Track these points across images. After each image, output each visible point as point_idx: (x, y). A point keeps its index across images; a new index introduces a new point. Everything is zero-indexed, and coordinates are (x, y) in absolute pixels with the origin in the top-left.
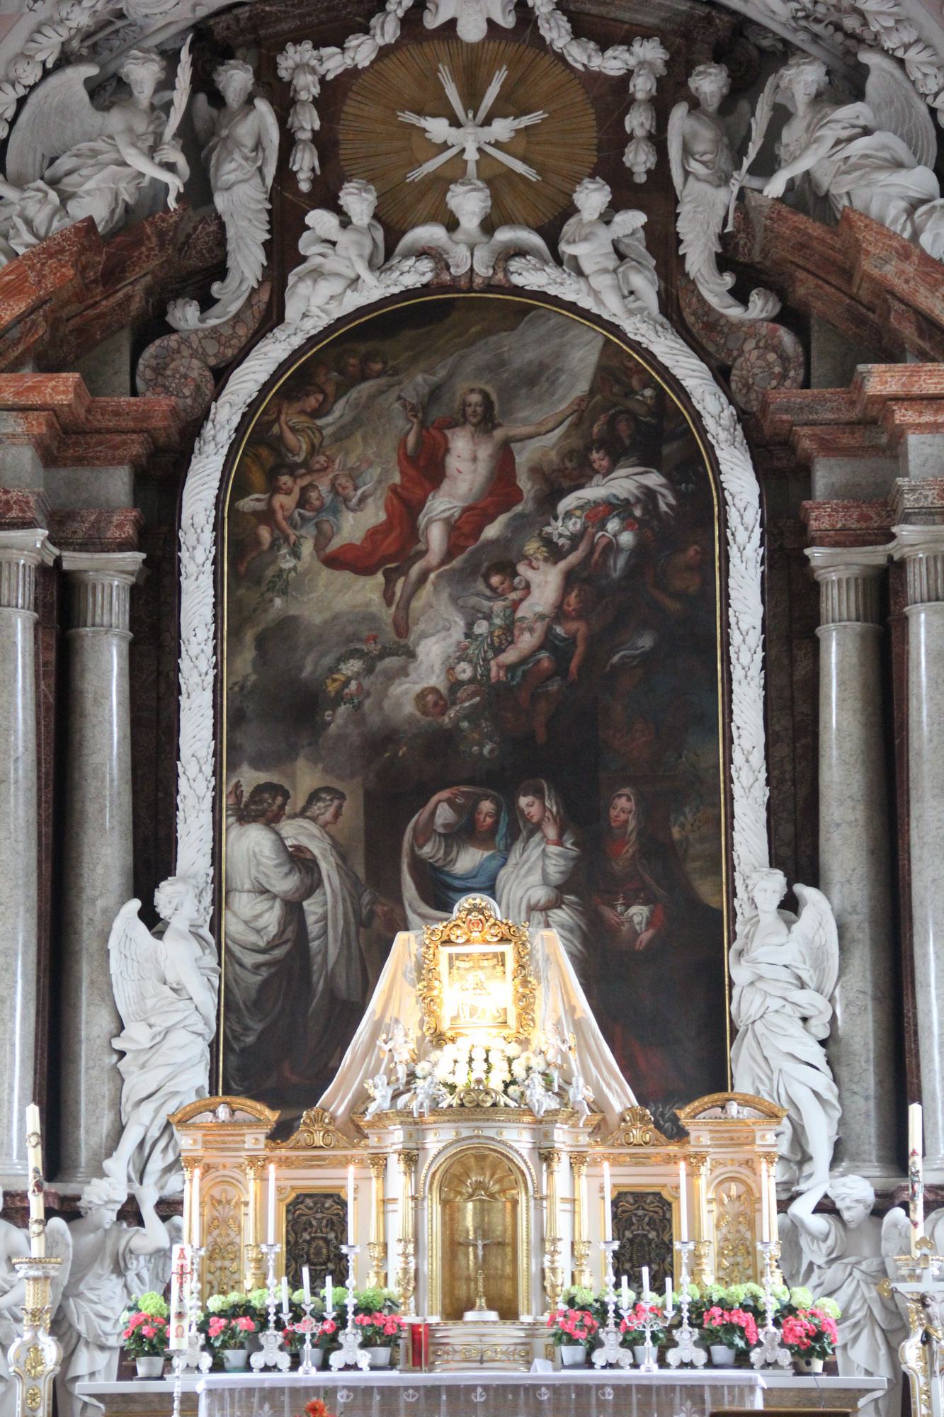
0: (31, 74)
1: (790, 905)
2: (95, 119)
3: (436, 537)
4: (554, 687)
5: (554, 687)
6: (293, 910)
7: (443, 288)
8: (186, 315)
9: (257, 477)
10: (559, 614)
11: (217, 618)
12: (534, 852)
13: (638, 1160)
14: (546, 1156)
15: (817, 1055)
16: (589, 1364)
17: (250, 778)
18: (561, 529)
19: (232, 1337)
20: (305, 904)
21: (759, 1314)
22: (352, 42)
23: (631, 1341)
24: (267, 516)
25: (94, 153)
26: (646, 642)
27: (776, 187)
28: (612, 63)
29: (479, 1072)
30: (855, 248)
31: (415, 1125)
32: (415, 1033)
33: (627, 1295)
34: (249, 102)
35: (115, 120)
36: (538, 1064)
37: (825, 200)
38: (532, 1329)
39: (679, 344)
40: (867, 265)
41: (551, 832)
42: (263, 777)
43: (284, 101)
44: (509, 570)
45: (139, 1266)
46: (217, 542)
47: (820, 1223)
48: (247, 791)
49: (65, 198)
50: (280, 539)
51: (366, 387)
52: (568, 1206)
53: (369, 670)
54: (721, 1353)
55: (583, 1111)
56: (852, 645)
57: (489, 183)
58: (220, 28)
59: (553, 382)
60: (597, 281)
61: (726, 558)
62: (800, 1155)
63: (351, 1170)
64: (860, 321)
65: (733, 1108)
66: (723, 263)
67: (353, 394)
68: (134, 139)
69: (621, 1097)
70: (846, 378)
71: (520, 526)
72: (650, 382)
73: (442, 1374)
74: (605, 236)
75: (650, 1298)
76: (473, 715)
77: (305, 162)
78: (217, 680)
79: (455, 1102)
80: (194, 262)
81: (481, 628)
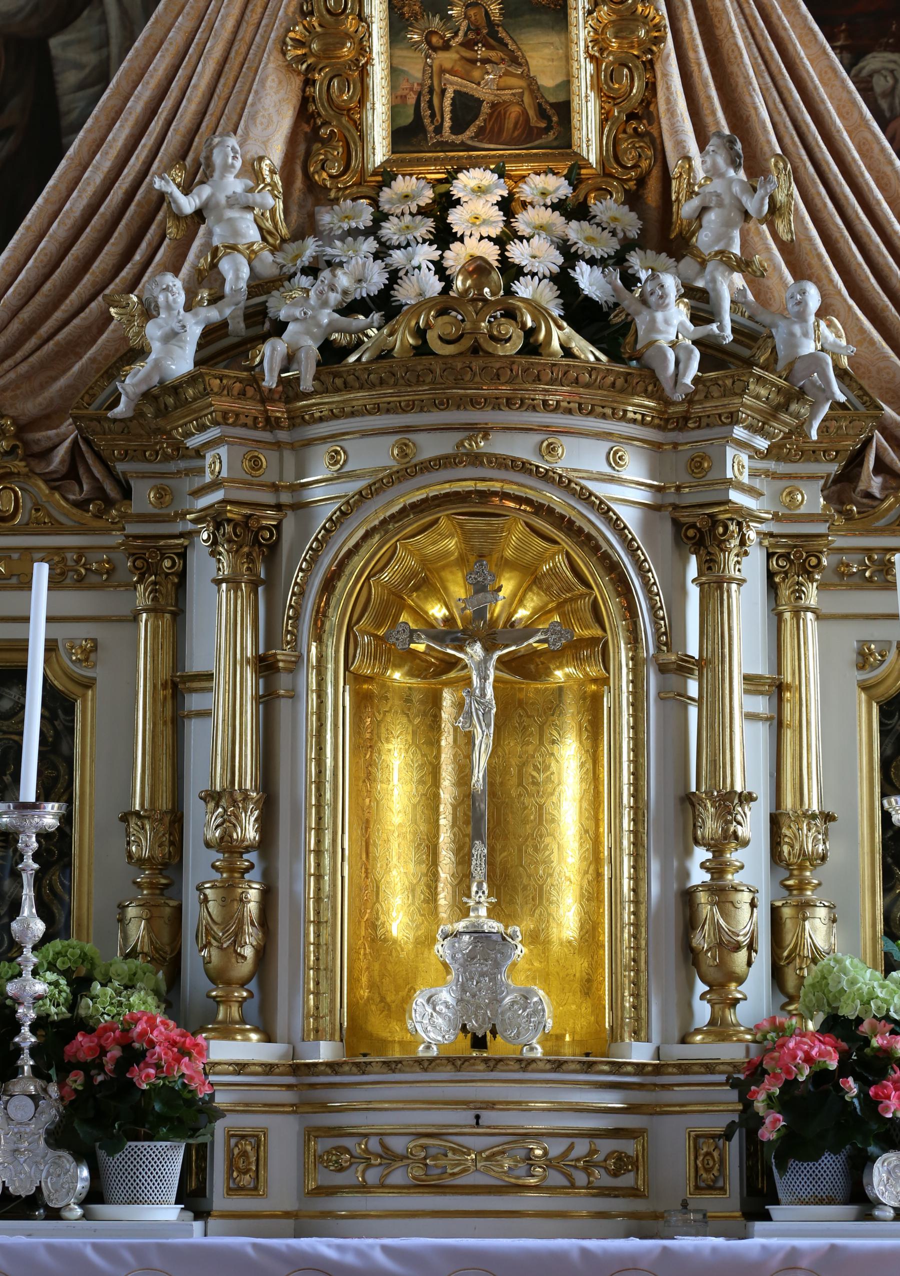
20: (54, 43)
52: (760, 704)
55: (826, 391)
79: (403, 339)
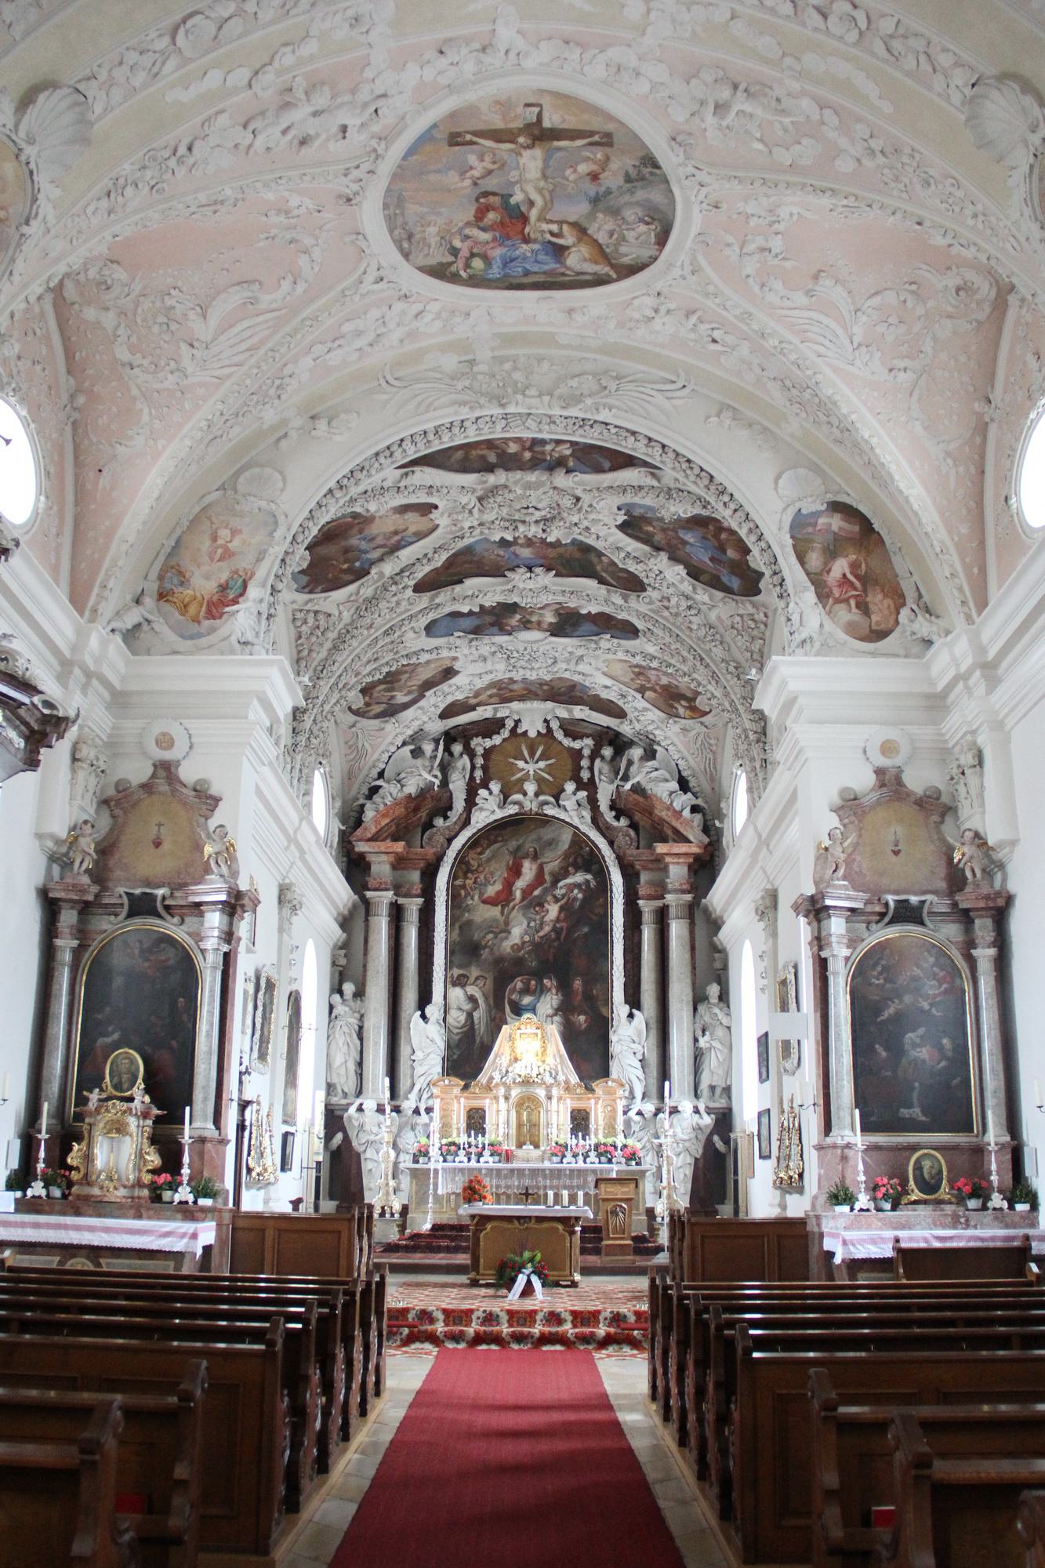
0: (393, 749)
1: (631, 1016)
2: (414, 761)
3: (518, 894)
4: (555, 944)
5: (555, 944)
6: (470, 1015)
7: (522, 814)
8: (439, 822)
9: (460, 874)
10: (558, 920)
11: (447, 920)
12: (548, 997)
13: (579, 1099)
14: (549, 1098)
15: (638, 1065)
16: (562, 1162)
17: (456, 972)
18: (559, 892)
19: (449, 1152)
21: (615, 1147)
22: (494, 737)
23: (575, 1156)
24: (464, 887)
25: (412, 772)
26: (586, 930)
27: (628, 786)
28: (577, 745)
29: (529, 1071)
30: (652, 806)
31: (508, 1088)
32: (508, 1058)
33: (574, 1141)
34: (461, 755)
35: (419, 762)
36: (548, 1068)
37: (644, 790)
38: (544, 1152)
39: (598, 834)
40: (656, 812)
41: (554, 991)
42: (461, 972)
43: (472, 755)
44: (541, 905)
45: (419, 1128)
46: (447, 895)
47: (637, 1118)
48: (455, 976)
49: (402, 786)
50: (468, 894)
51: (497, 845)
53: (496, 937)
54: (603, 1159)
56: (652, 932)
57: (537, 781)
58: (452, 732)
59: (557, 845)
60: (571, 813)
61: (612, 903)
62: (632, 1096)
63: (487, 1101)
64: (654, 827)
65: (610, 1083)
66: (612, 808)
67: (492, 848)
68: (425, 767)
69: (574, 1079)
70: (650, 847)
71: (545, 891)
72: (588, 845)
73: (515, 1165)
74: (574, 799)
75: (581, 1142)
76: (529, 953)
77: (478, 774)
78: (447, 940)
80: (442, 805)
81: (532, 924)
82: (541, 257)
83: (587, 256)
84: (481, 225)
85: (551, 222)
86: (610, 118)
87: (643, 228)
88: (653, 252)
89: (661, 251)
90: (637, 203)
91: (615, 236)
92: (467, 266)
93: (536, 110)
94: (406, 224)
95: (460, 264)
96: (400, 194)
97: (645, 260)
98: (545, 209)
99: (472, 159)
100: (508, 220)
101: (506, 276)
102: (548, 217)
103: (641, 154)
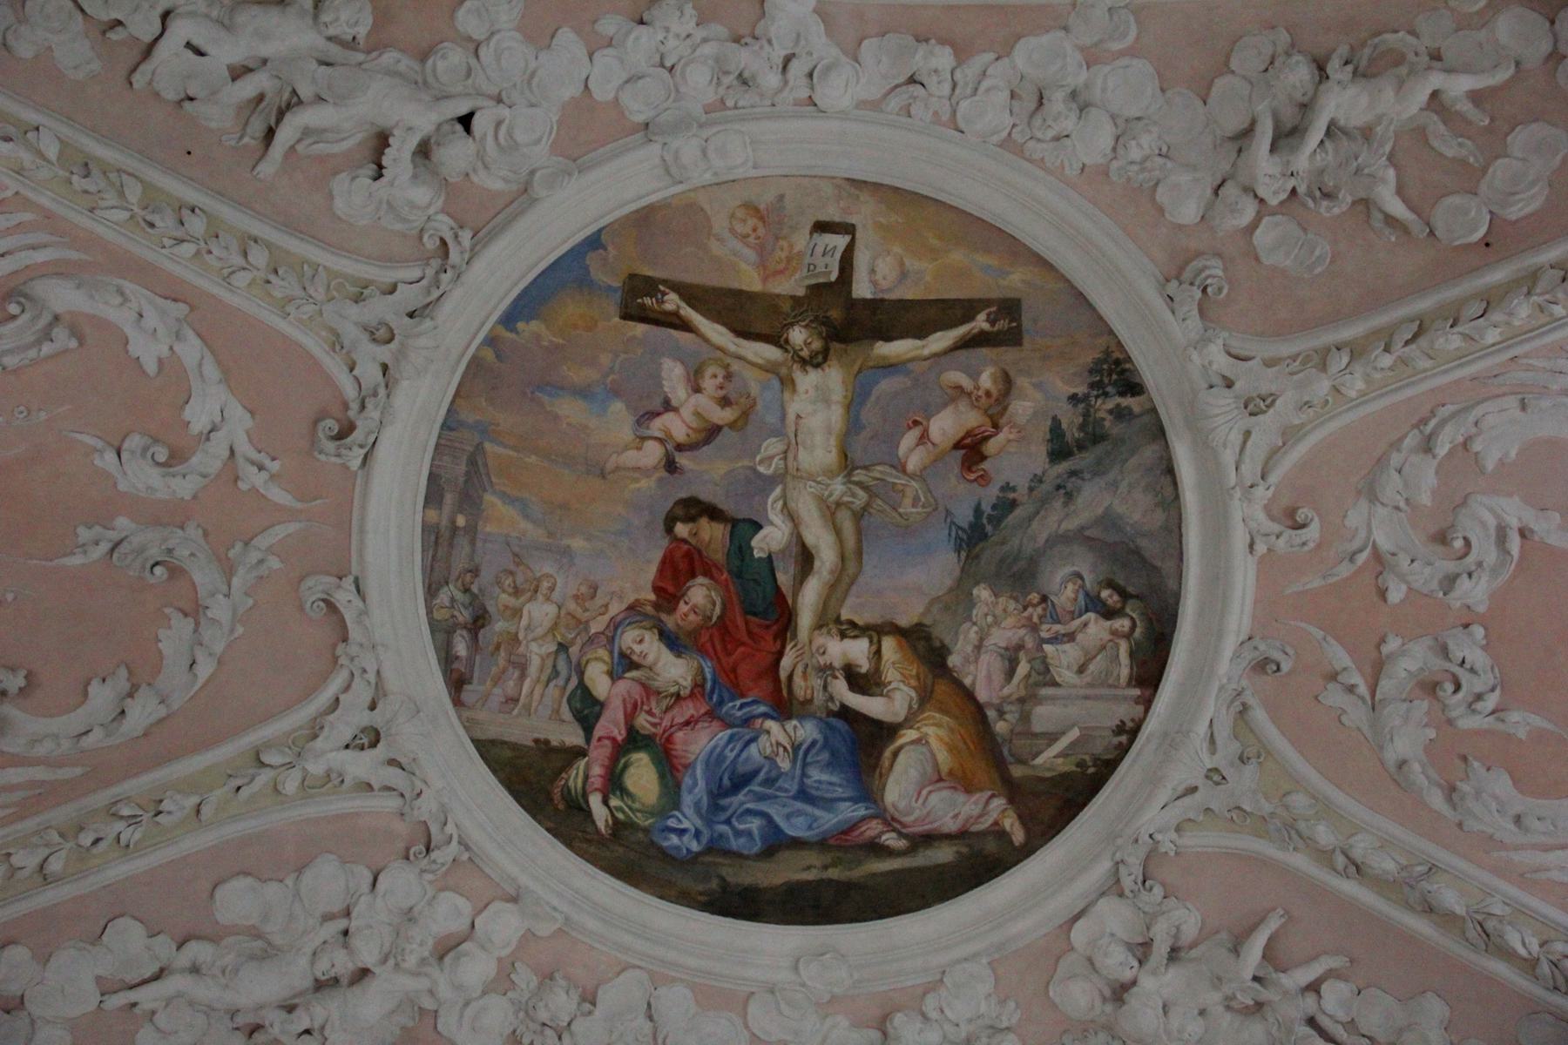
82: (816, 775)
83: (943, 757)
84: (670, 621)
85: (850, 630)
86: (1016, 250)
87: (1096, 629)
88: (1125, 711)
89: (1148, 703)
90: (1080, 537)
91: (1023, 669)
92: (614, 783)
93: (841, 241)
94: (475, 572)
95: (595, 766)
96: (479, 447)
97: (1102, 745)
98: (839, 585)
99: (673, 376)
100: (740, 621)
101: (715, 848)
102: (845, 615)
103: (1088, 358)
